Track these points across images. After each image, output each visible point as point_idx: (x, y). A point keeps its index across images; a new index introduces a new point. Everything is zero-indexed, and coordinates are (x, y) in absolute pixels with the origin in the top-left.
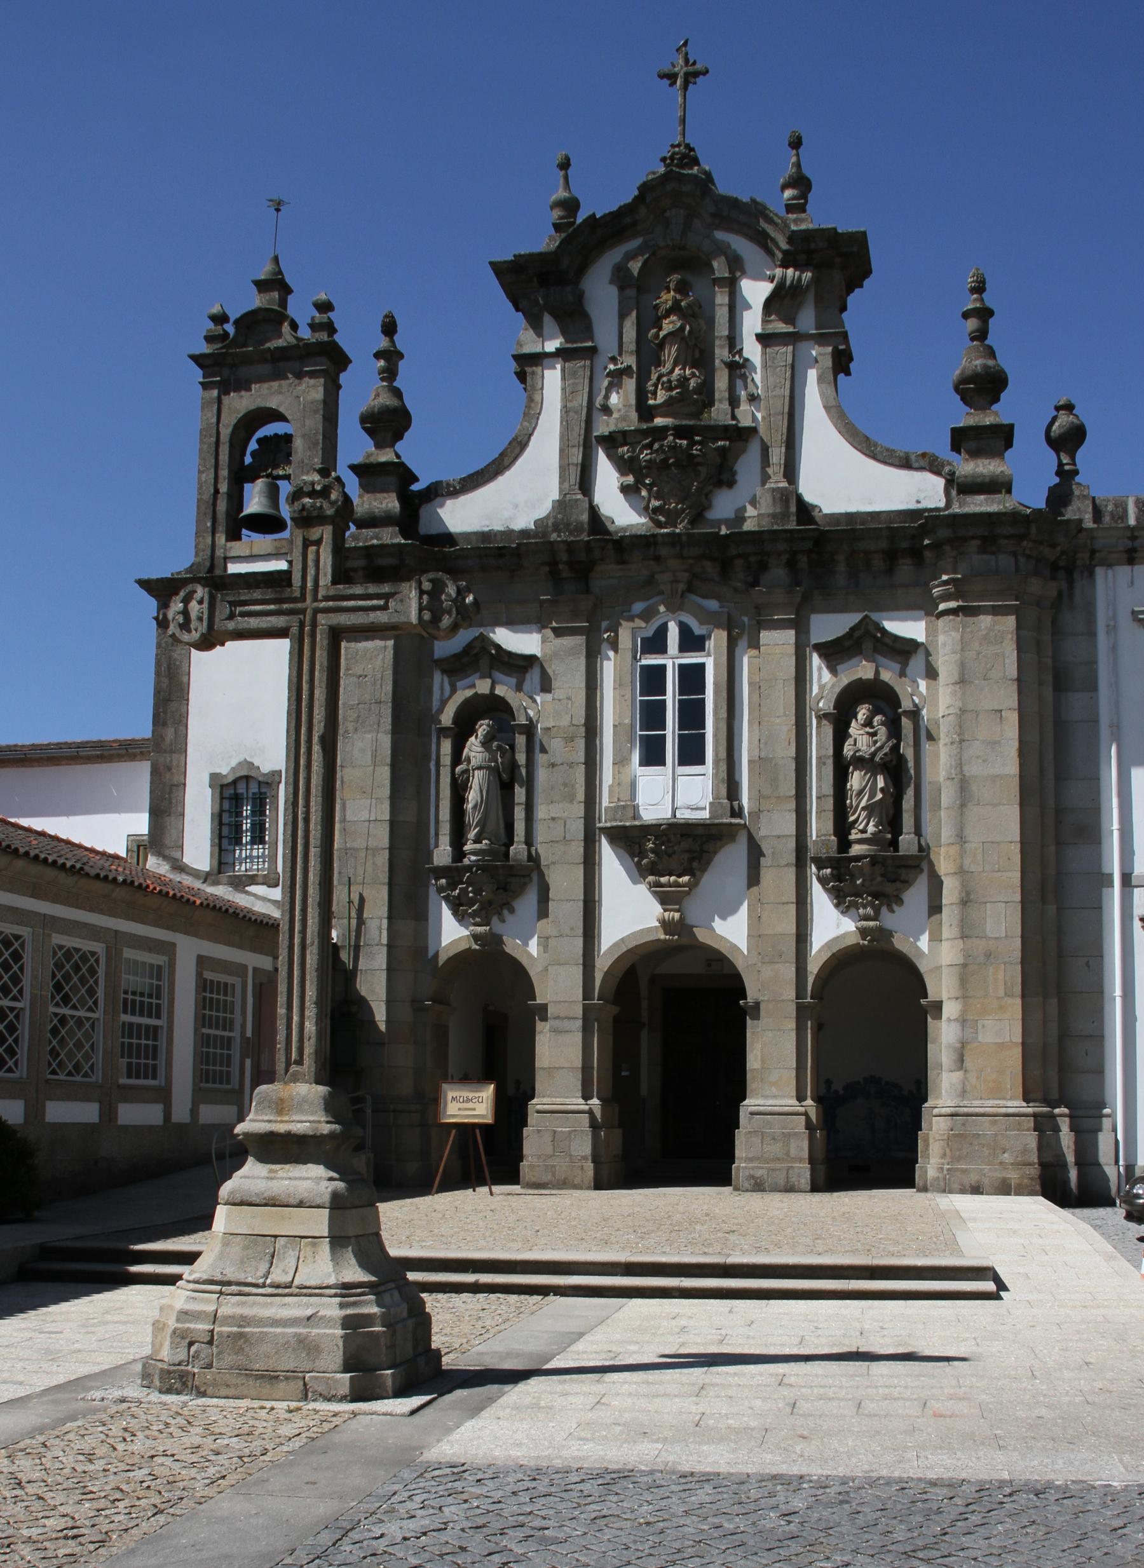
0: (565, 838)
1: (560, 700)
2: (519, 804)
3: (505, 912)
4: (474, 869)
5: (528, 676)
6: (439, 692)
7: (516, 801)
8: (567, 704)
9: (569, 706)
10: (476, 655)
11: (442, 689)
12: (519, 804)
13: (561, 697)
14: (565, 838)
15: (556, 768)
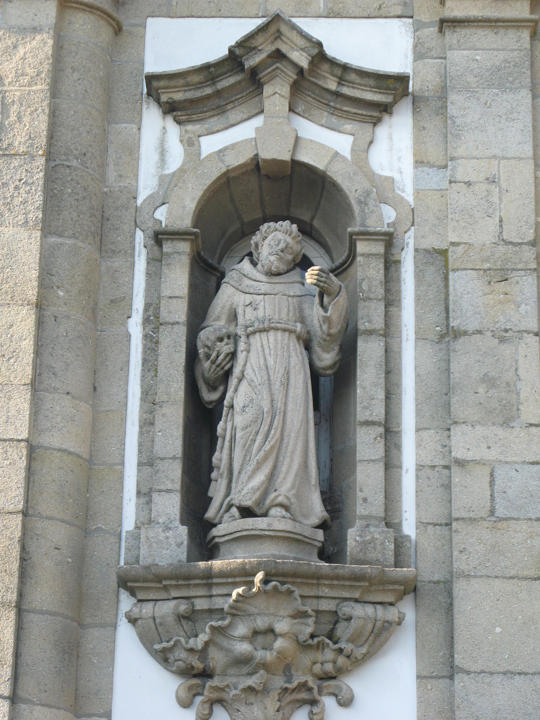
0: (492, 512)
1: (469, 184)
2: (367, 423)
3: (329, 702)
4: (260, 576)
5: (382, 131)
6: (156, 157)
7: (361, 414)
8: (489, 192)
9: (495, 199)
10: (254, 72)
11: (163, 152)
12: (367, 423)
13: (473, 178)
14: (492, 512)
15: (462, 340)
